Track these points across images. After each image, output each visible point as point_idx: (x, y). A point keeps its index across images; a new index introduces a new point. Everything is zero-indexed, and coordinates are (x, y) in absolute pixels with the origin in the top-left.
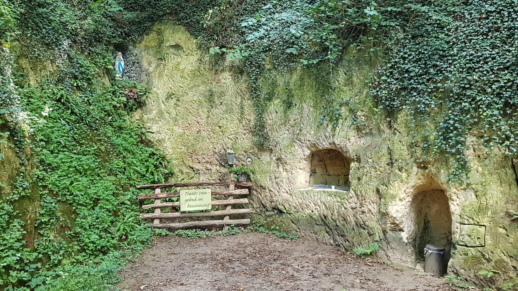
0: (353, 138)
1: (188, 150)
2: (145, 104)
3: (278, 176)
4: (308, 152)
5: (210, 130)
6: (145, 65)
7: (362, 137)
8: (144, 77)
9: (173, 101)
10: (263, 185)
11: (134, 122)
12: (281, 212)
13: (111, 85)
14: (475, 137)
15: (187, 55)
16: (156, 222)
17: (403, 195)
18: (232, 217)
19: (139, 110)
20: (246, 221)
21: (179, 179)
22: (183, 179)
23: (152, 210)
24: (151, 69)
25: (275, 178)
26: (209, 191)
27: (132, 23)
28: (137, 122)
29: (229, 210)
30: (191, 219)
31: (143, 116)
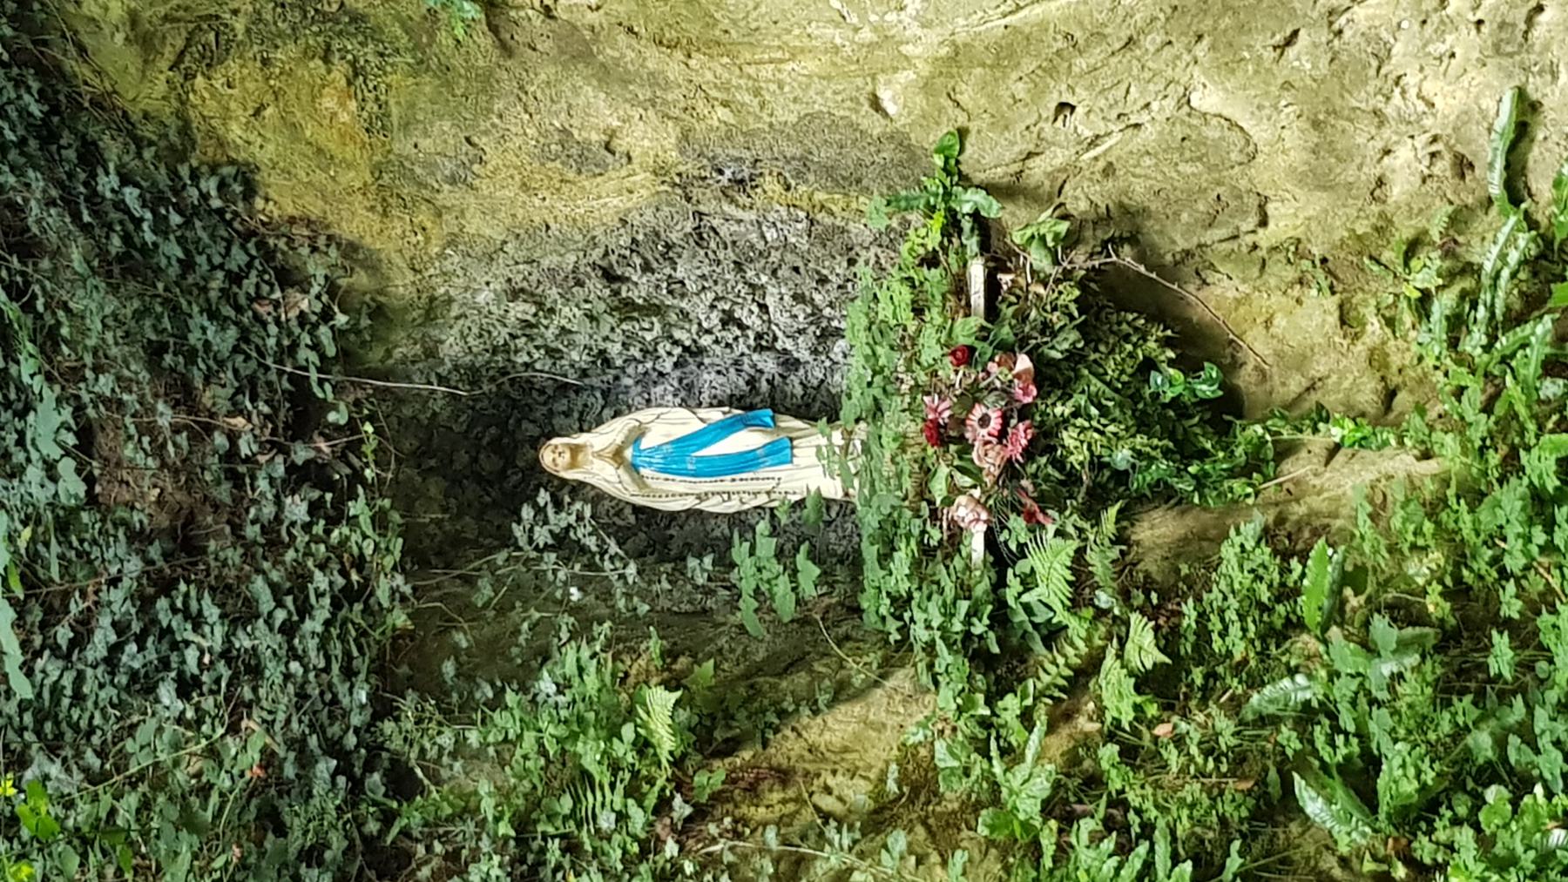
11: (1377, 360)
13: (900, 679)
28: (1374, 327)
31: (1297, 249)
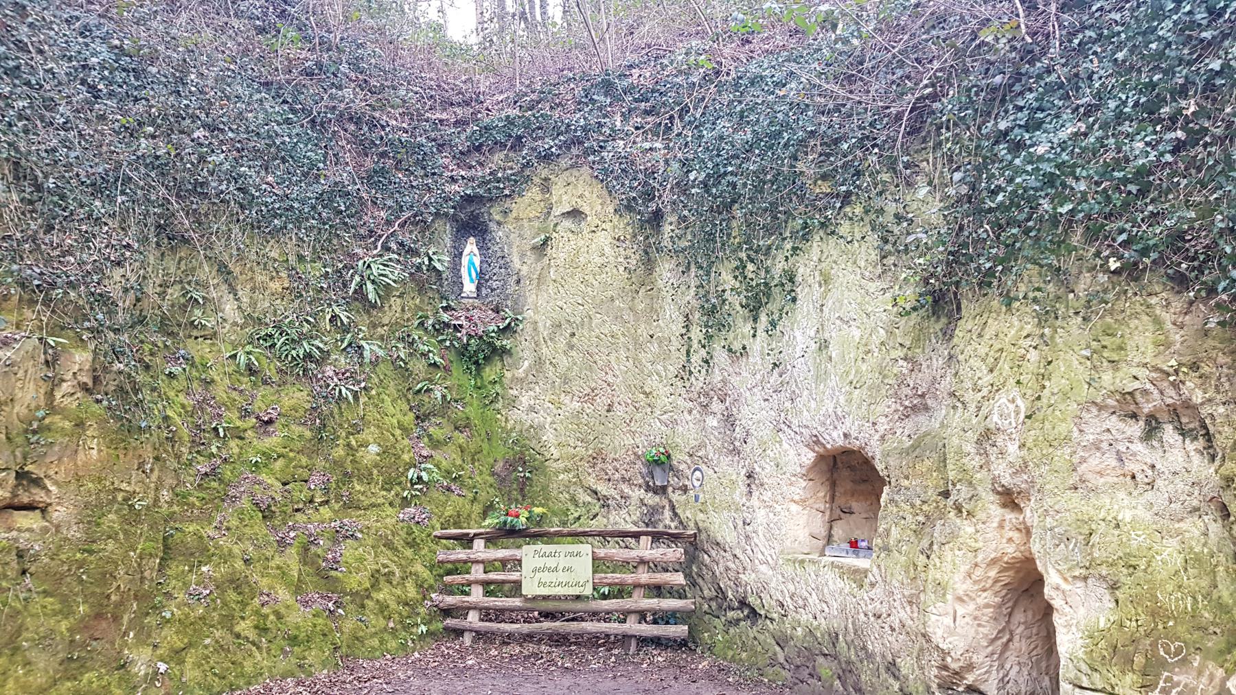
0: (883, 420)
1: (587, 450)
3: (749, 518)
4: (809, 457)
5: (629, 401)
7: (907, 417)
8: (511, 288)
10: (719, 539)
12: (754, 614)
14: (1114, 418)
15: (594, 231)
17: (962, 587)
21: (571, 517)
22: (579, 518)
25: (744, 523)
26: (586, 549)
30: (549, 615)
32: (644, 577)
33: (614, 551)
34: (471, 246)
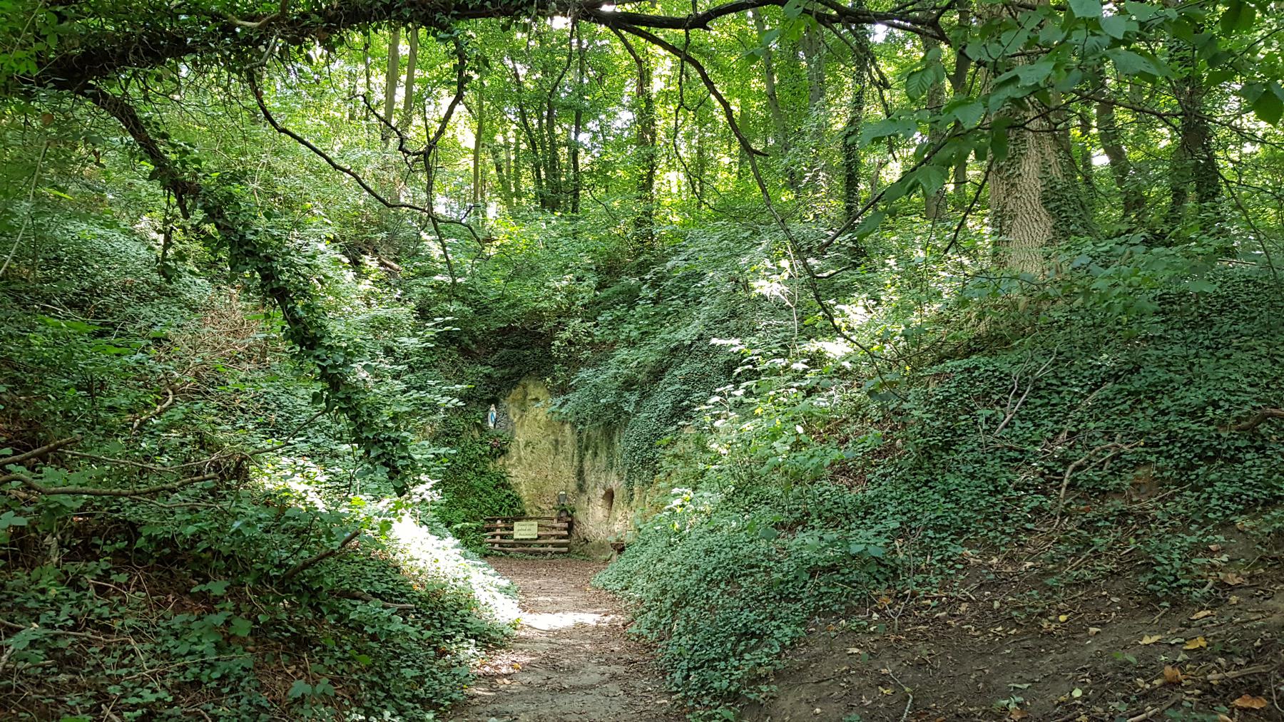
2: (507, 452)
4: (603, 492)
6: (511, 415)
8: (509, 427)
9: (529, 449)
16: (496, 546)
18: (554, 545)
19: (503, 457)
20: (565, 549)
23: (494, 537)
24: (515, 420)
26: (536, 523)
27: (502, 378)
29: (553, 540)
30: (525, 545)
32: (554, 532)
33: (544, 522)
34: (493, 408)
